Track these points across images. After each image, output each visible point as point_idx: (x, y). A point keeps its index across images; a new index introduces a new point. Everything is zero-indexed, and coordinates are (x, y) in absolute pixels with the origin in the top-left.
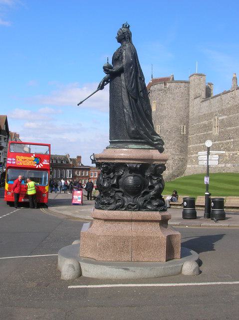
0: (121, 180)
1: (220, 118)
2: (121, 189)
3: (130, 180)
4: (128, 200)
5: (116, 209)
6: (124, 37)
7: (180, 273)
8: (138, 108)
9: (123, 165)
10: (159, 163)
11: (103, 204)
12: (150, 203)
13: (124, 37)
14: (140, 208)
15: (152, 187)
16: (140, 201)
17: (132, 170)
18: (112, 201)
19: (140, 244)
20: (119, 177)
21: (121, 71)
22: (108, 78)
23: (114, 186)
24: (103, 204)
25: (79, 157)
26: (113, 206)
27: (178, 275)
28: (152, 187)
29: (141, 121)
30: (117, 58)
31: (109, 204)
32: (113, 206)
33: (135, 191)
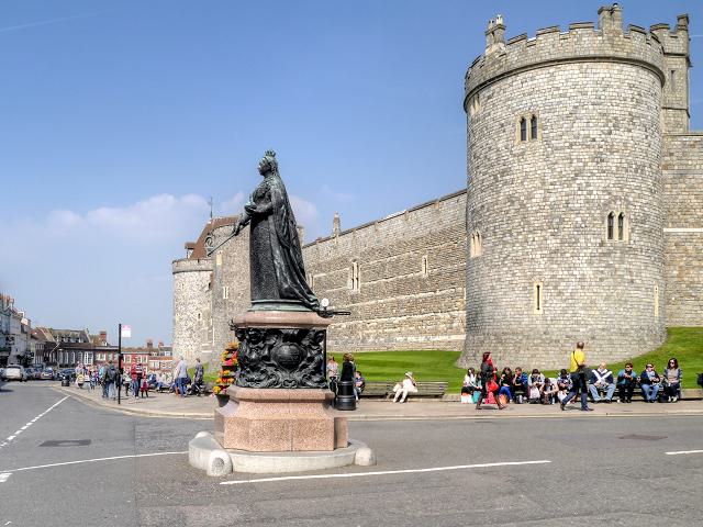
0: (273, 350)
1: (315, 276)
2: (273, 362)
3: (286, 350)
4: (282, 375)
5: (268, 387)
6: (268, 170)
7: (353, 463)
8: (291, 260)
9: (275, 332)
10: (319, 329)
11: (252, 380)
12: (310, 378)
13: (268, 170)
14: (301, 384)
15: (311, 359)
16: (297, 376)
17: (288, 338)
18: (263, 377)
19: (302, 429)
20: (271, 347)
21: (270, 212)
22: (246, 221)
23: (266, 358)
24: (252, 380)
25: (103, 334)
26: (265, 383)
27: (352, 465)
28: (311, 359)
29: (296, 277)
30: (261, 196)
31: (260, 381)
32: (265, 383)
33: (290, 365)
